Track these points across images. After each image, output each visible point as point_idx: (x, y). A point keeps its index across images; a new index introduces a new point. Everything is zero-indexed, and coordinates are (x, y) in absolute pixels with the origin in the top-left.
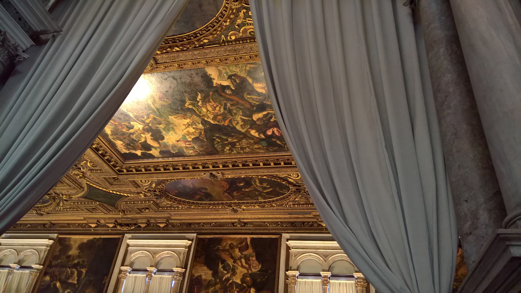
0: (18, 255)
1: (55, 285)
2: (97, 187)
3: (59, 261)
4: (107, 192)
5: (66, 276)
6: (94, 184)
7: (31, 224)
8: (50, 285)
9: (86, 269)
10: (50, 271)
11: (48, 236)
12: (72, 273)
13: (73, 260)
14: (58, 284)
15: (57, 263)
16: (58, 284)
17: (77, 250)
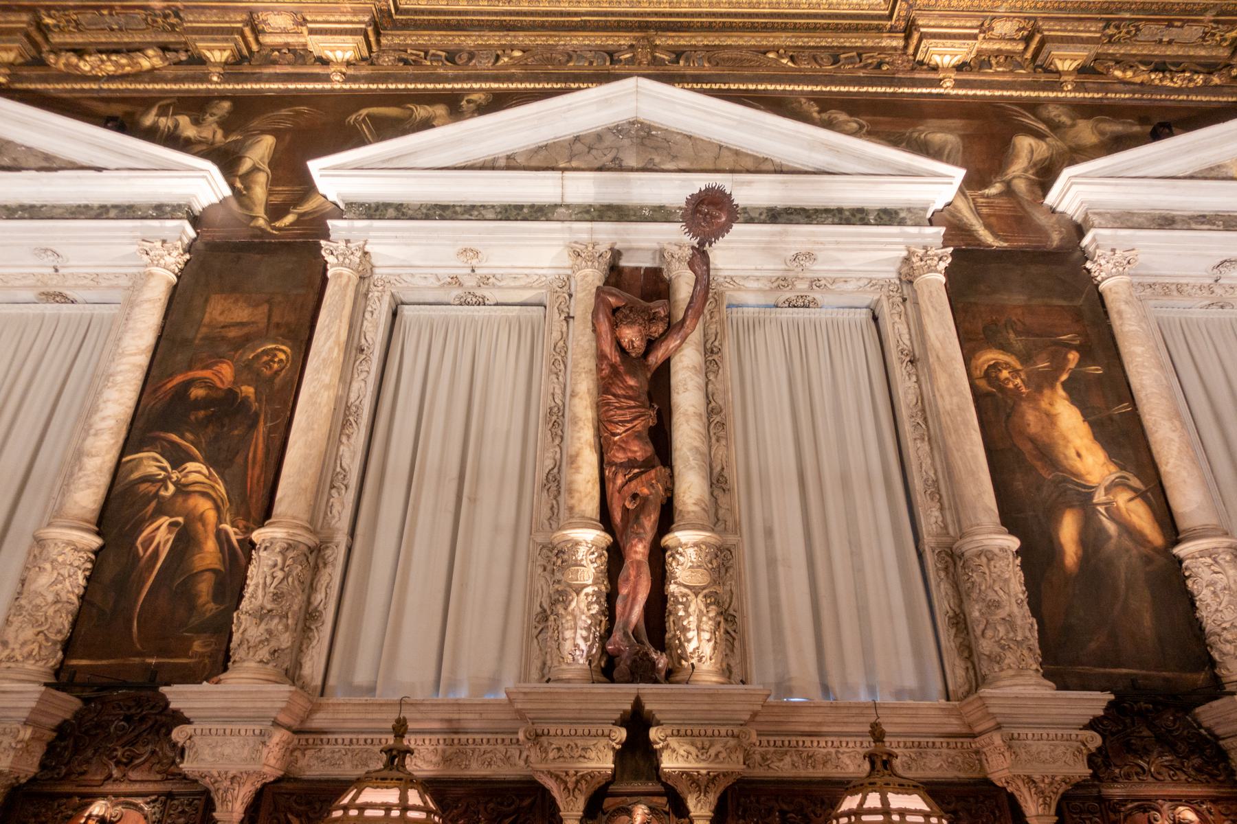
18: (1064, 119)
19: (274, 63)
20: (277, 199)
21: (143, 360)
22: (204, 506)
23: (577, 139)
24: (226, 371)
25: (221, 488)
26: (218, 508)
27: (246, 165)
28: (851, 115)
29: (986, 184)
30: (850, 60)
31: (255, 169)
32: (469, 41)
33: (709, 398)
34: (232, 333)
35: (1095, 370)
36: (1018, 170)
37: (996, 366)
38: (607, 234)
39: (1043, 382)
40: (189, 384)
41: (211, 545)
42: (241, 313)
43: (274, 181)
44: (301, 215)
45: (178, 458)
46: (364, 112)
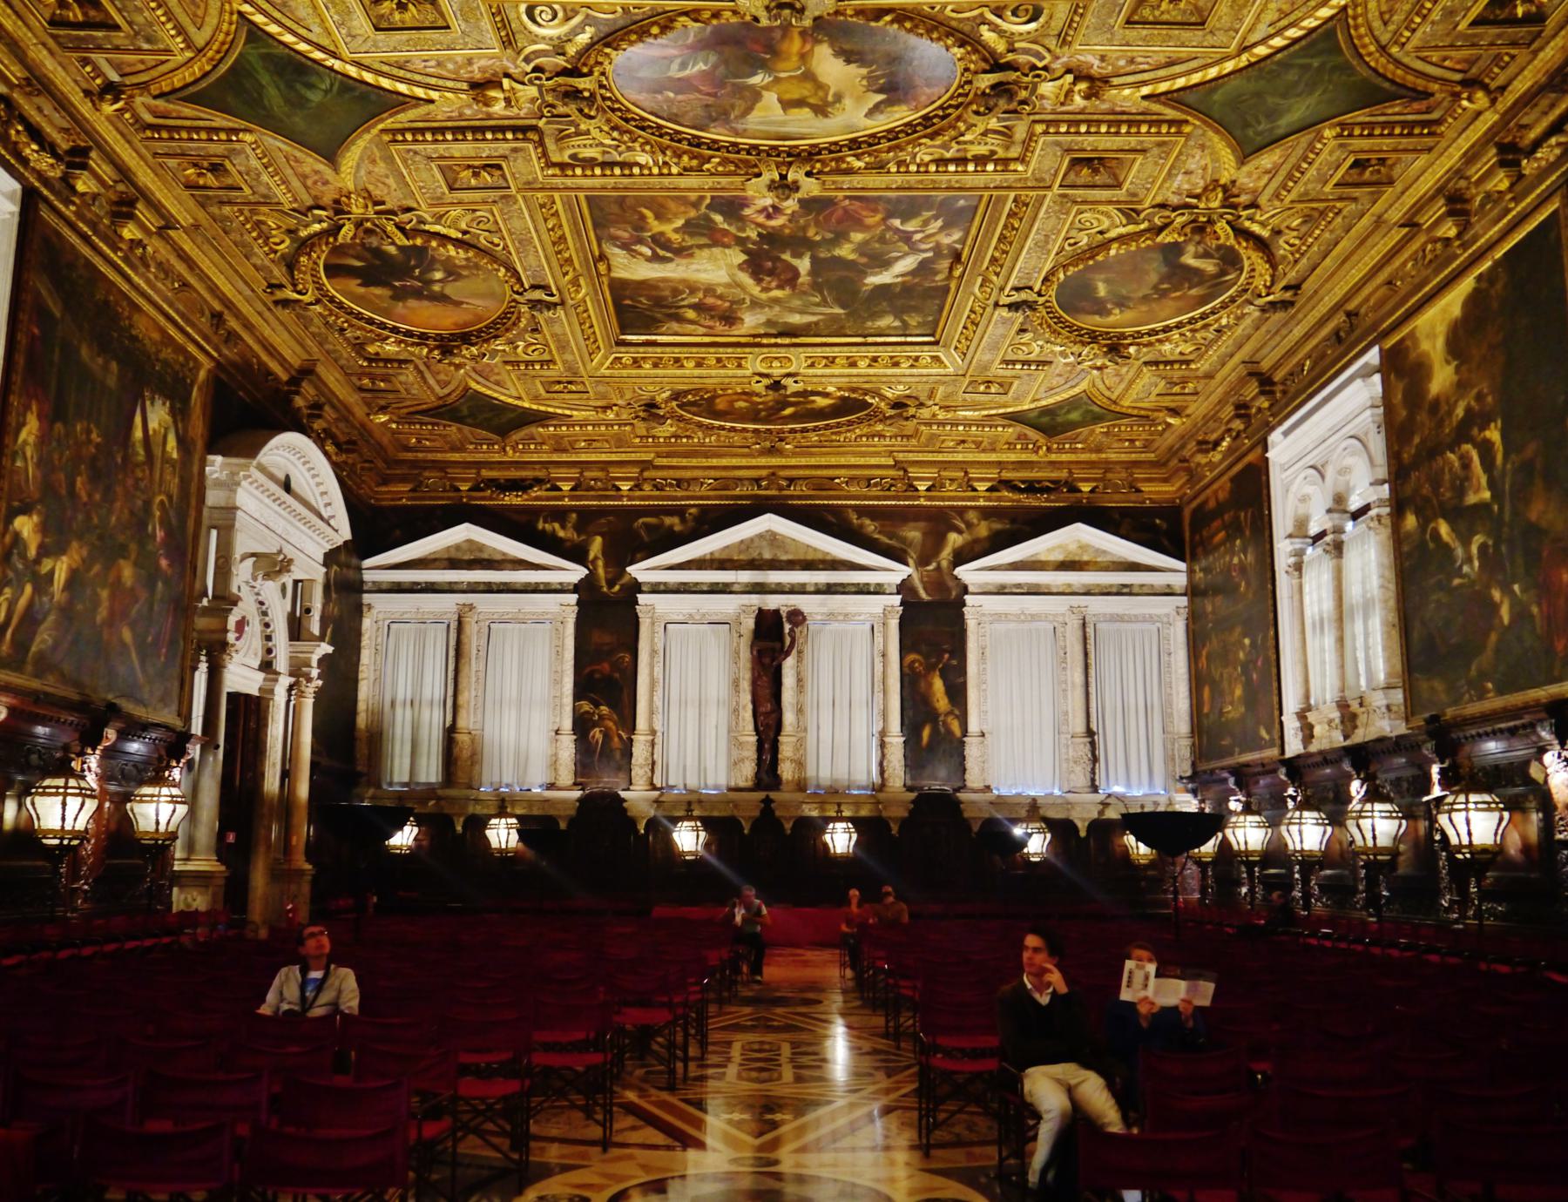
0: (1323, 477)
1: (1436, 535)
2: (1196, 78)
3: (1417, 440)
4: (1251, 65)
5: (1453, 487)
6: (1174, 77)
7: (1308, 356)
8: (1423, 543)
9: (1499, 422)
10: (1408, 490)
11: (1366, 364)
12: (1466, 464)
13: (1450, 413)
14: (1444, 529)
15: (1413, 451)
16: (1444, 529)
17: (1448, 362)
18: (975, 521)
19: (592, 489)
20: (610, 576)
21: (572, 662)
22: (610, 724)
23: (742, 541)
24: (606, 666)
25: (615, 717)
26: (615, 723)
27: (591, 556)
28: (873, 520)
29: (928, 564)
30: (876, 485)
31: (596, 558)
32: (688, 474)
33: (798, 674)
34: (606, 648)
35: (954, 662)
36: (946, 554)
37: (913, 662)
38: (755, 600)
39: (930, 668)
40: (592, 672)
41: (616, 739)
42: (607, 639)
43: (606, 566)
44: (622, 586)
45: (597, 705)
46: (641, 521)
